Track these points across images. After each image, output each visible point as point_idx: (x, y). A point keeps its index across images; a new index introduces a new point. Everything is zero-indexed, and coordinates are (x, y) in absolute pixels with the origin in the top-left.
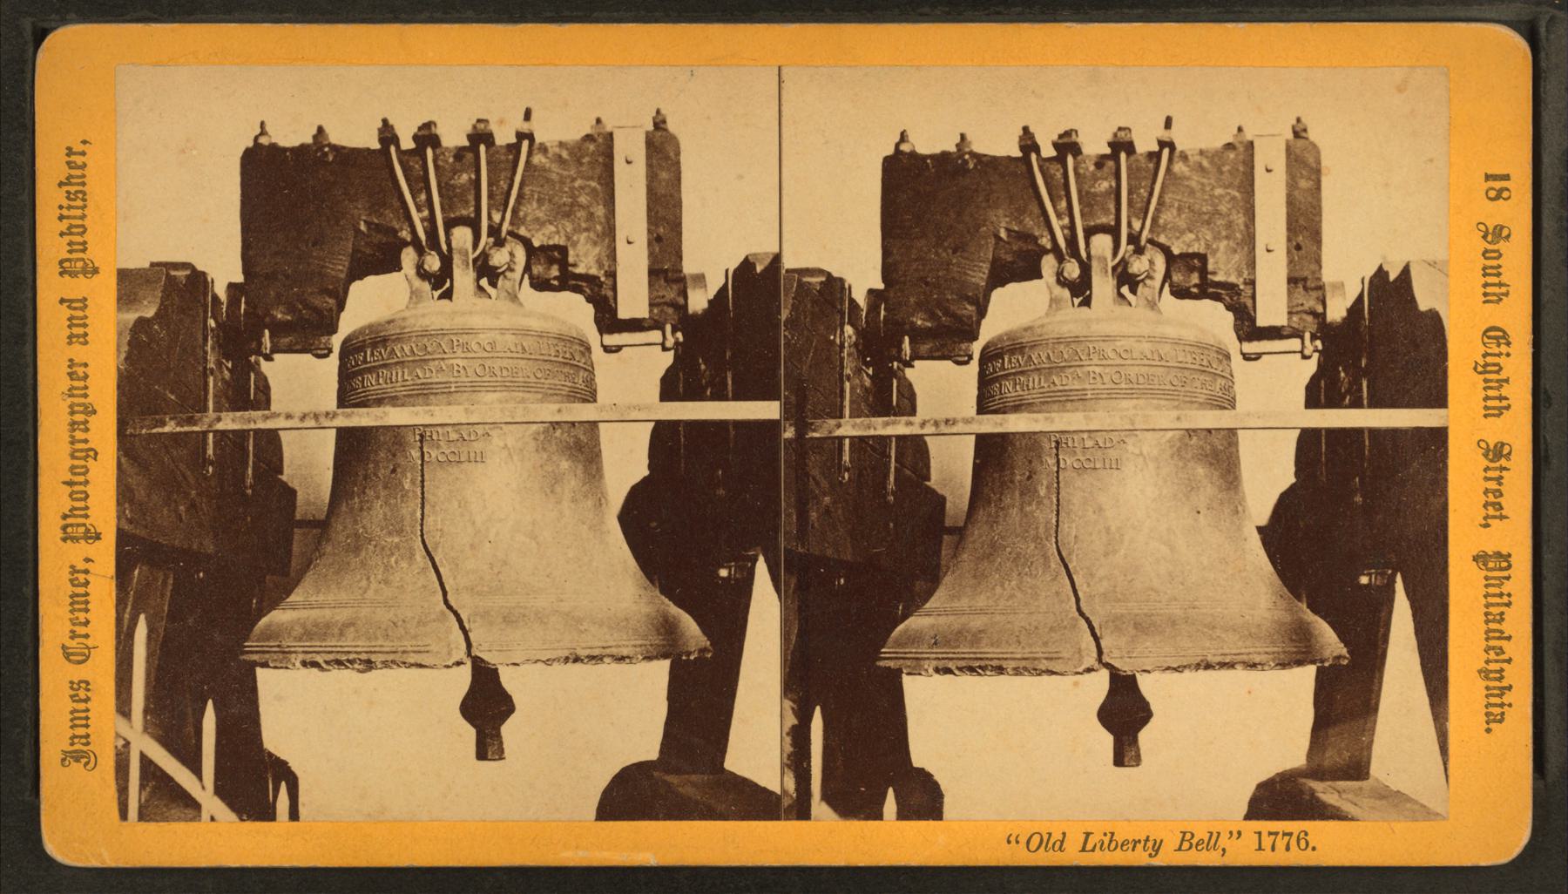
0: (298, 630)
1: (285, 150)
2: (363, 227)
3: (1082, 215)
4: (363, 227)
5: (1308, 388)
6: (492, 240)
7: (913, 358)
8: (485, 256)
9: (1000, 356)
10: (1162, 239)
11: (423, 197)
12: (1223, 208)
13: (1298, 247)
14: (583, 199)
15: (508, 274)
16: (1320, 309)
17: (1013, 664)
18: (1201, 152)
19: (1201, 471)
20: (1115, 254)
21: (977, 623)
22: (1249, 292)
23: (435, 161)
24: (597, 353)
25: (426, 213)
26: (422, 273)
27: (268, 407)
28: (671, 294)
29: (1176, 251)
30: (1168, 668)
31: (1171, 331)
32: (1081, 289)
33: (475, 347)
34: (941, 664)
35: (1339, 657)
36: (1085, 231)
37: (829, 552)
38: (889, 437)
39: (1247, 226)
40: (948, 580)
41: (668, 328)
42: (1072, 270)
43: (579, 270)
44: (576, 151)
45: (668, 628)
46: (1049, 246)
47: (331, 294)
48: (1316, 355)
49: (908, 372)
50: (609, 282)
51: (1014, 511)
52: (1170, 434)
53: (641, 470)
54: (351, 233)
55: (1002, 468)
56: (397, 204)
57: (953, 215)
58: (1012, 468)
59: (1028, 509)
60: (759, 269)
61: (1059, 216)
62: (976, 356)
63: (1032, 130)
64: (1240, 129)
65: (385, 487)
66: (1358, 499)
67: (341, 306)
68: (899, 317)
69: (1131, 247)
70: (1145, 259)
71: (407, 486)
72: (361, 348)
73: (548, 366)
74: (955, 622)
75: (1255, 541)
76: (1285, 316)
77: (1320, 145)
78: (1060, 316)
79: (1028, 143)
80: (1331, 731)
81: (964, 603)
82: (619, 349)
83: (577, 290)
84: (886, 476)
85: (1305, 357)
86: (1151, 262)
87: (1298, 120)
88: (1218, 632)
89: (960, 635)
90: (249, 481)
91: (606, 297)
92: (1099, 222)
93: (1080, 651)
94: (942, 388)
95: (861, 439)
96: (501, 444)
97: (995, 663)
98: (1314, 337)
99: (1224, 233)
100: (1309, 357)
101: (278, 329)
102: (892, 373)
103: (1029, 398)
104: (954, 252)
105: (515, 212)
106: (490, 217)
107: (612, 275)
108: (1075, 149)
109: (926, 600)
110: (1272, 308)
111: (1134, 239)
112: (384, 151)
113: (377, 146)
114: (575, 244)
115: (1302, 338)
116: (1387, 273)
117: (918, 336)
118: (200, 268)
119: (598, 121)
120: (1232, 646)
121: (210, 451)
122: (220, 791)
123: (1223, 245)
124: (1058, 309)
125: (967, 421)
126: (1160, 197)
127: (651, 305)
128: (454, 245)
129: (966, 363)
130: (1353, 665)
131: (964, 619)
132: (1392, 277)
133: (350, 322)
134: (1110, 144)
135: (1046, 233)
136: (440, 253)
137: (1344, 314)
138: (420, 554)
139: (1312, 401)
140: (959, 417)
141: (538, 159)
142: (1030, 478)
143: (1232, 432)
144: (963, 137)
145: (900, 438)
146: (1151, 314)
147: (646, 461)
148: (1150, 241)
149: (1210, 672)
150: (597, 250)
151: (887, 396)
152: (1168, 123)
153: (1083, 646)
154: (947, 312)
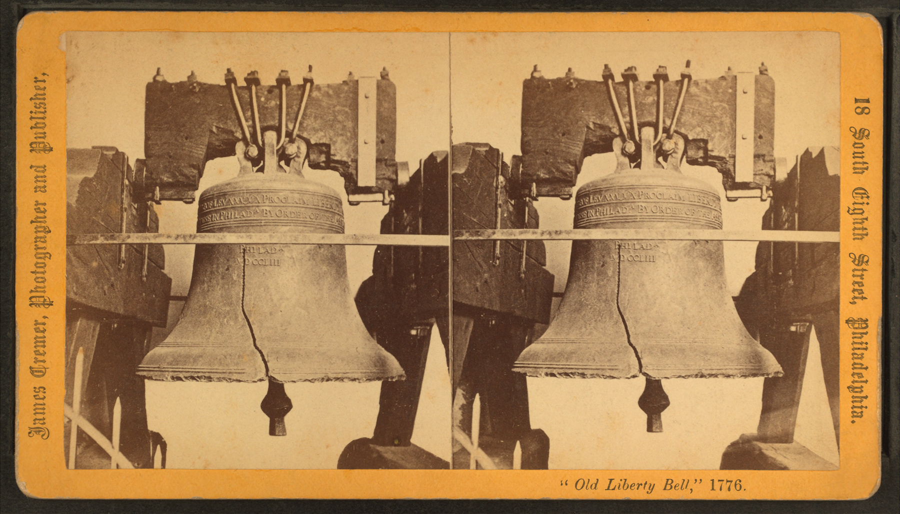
0: (170, 359)
1: (172, 84)
2: (214, 130)
3: (637, 116)
4: (214, 130)
5: (764, 218)
6: (288, 139)
7: (538, 195)
8: (283, 148)
9: (587, 195)
10: (683, 131)
11: (249, 113)
12: (718, 114)
13: (760, 137)
14: (340, 118)
15: (296, 159)
16: (772, 173)
17: (591, 372)
18: (706, 81)
19: (701, 264)
20: (655, 138)
21: (569, 348)
22: (732, 161)
23: (256, 93)
24: (345, 204)
25: (250, 123)
26: (247, 157)
27: (156, 229)
28: (389, 173)
29: (690, 138)
30: (680, 377)
31: (687, 184)
32: (635, 158)
33: (276, 200)
34: (549, 371)
35: (778, 372)
36: (638, 125)
37: (486, 306)
38: (523, 240)
39: (732, 125)
40: (553, 324)
41: (387, 192)
42: (631, 147)
43: (336, 158)
44: (337, 89)
45: (381, 363)
46: (618, 133)
47: (193, 166)
48: (769, 199)
49: (535, 203)
50: (353, 165)
51: (594, 286)
52: (685, 242)
53: (368, 273)
54: (208, 133)
55: (587, 258)
56: (234, 116)
57: (563, 114)
58: (593, 260)
59: (602, 283)
60: (439, 160)
61: (624, 116)
62: (574, 195)
63: (610, 66)
64: (729, 69)
65: (223, 278)
66: (791, 282)
67: (201, 175)
68: (530, 172)
69: (665, 135)
70: (672, 141)
71: (235, 278)
72: (211, 199)
73: (315, 212)
74: (558, 348)
75: (731, 304)
76: (752, 176)
77: (774, 79)
78: (623, 173)
79: (608, 75)
80: (772, 415)
81: (562, 337)
82: (358, 203)
83: (335, 169)
84: (520, 263)
85: (762, 200)
86: (676, 144)
87: (763, 64)
88: (709, 357)
89: (561, 354)
90: (145, 273)
91: (352, 174)
92: (646, 120)
93: (629, 365)
94: (554, 213)
95: (507, 241)
96: (289, 255)
97: (580, 371)
98: (768, 189)
99: (718, 128)
100: (765, 200)
101: (164, 186)
102: (525, 204)
103: (604, 219)
104: (563, 135)
105: (301, 124)
106: (287, 126)
107: (355, 161)
108: (634, 78)
109: (542, 334)
110: (744, 172)
111: (666, 130)
112: (228, 87)
113: (224, 84)
114: (335, 143)
115: (761, 189)
116: (811, 154)
117: (540, 182)
118: (120, 150)
119: (351, 74)
120: (715, 364)
121: (123, 255)
122: (122, 449)
123: (718, 134)
124: (622, 169)
125: (568, 233)
126: (682, 106)
127: (377, 179)
128: (266, 141)
129: (568, 199)
130: (785, 378)
131: (563, 346)
132: (814, 156)
133: (205, 184)
134: (655, 76)
135: (616, 125)
136: (258, 145)
137: (786, 176)
138: (241, 316)
139: (766, 226)
140: (563, 229)
141: (315, 94)
142: (603, 266)
143: (720, 241)
144: (570, 70)
145: (529, 241)
146: (676, 173)
147: (372, 268)
148: (676, 132)
149: (703, 379)
150: (347, 147)
151: (522, 216)
152: (688, 64)
153: (632, 362)
154: (558, 170)
